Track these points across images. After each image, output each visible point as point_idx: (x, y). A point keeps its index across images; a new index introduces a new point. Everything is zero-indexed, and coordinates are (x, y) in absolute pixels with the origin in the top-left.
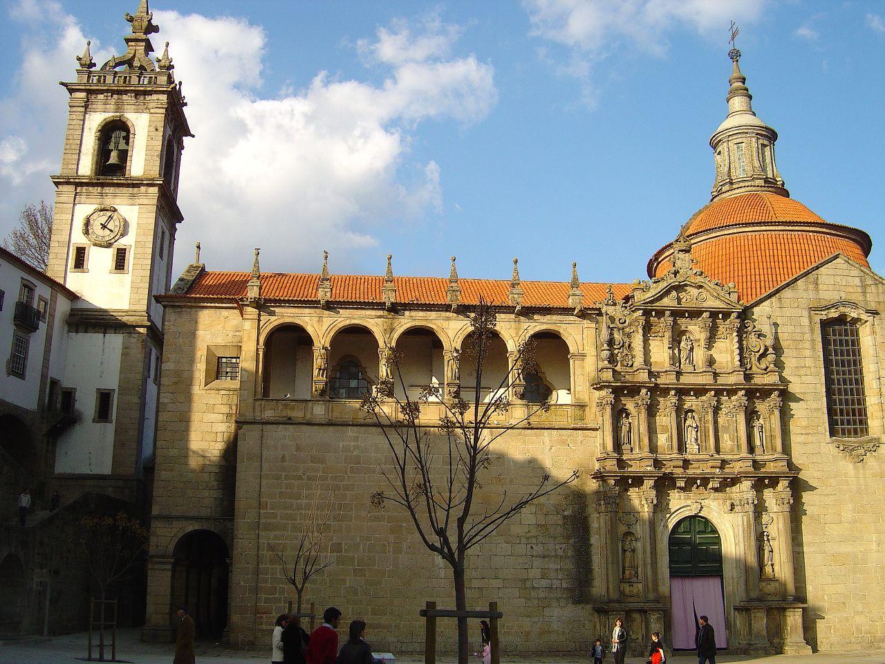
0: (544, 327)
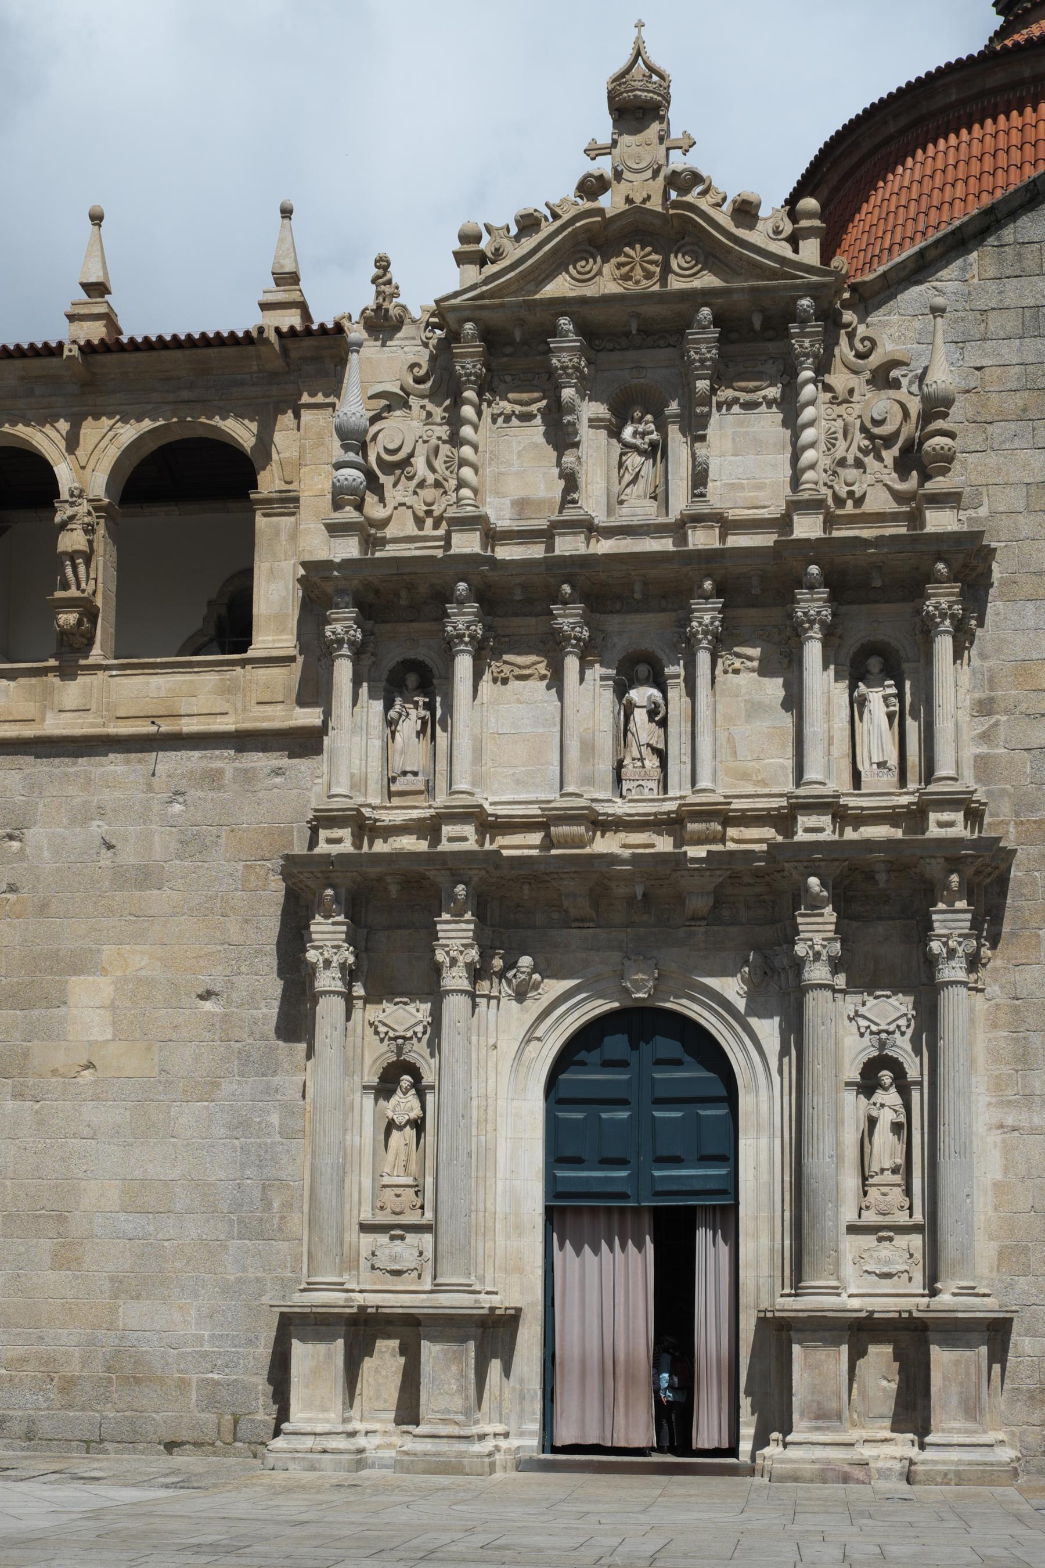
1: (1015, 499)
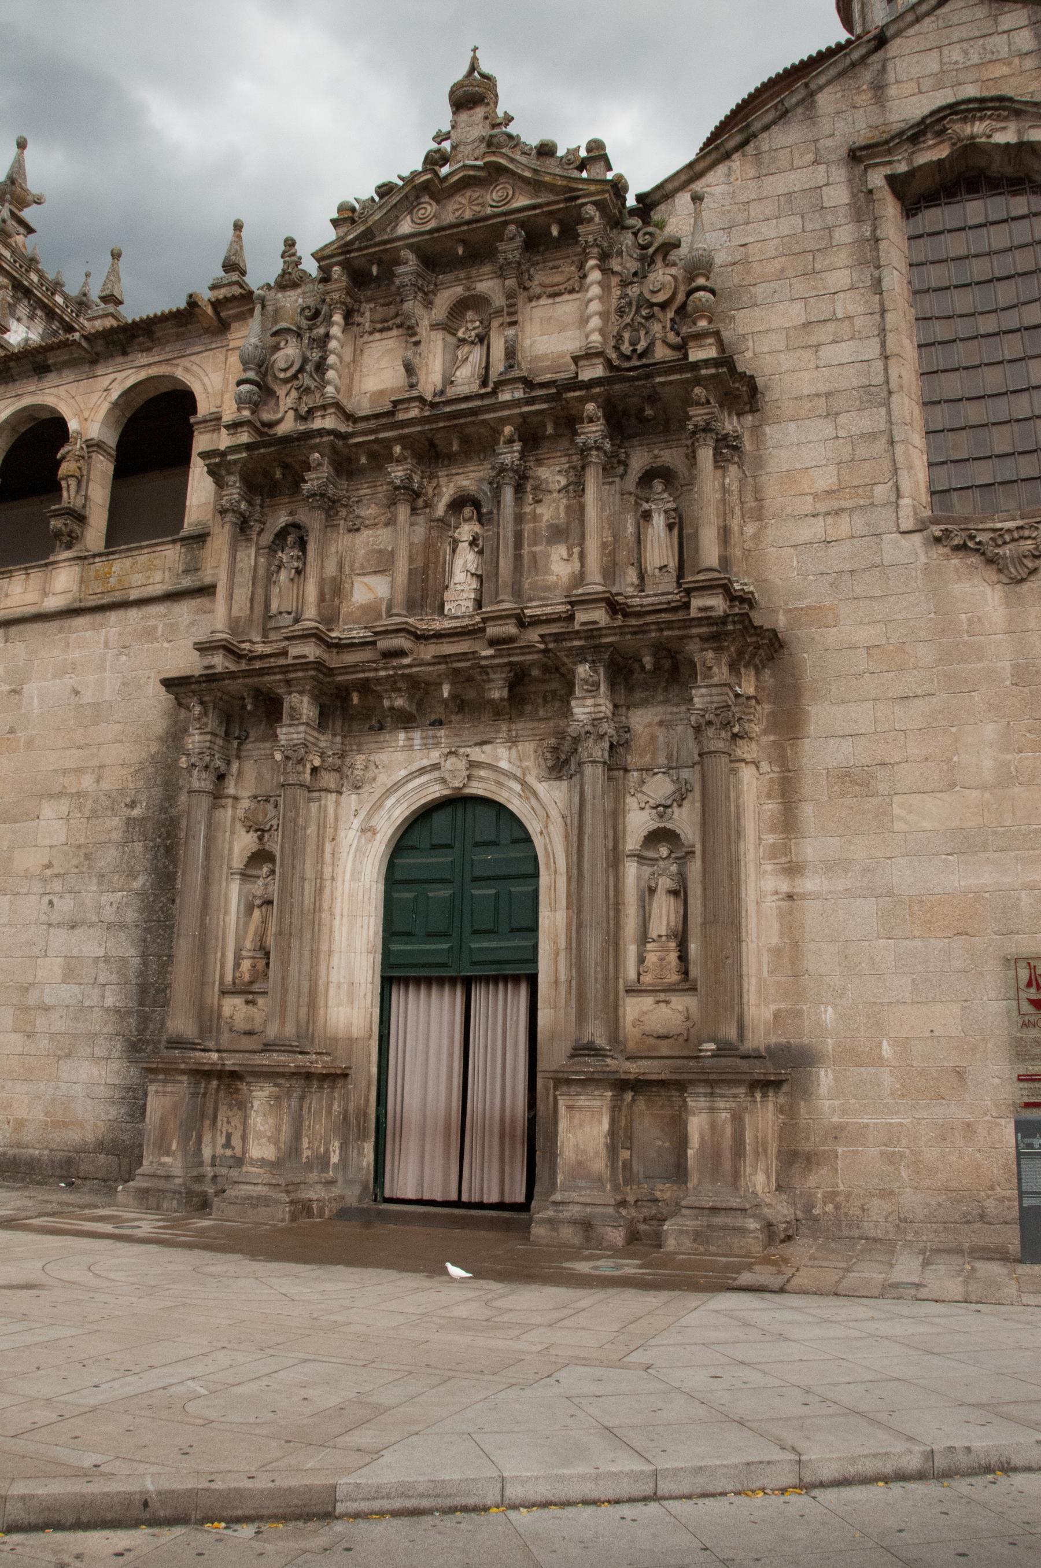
0: (143, 375)
1: (777, 341)
